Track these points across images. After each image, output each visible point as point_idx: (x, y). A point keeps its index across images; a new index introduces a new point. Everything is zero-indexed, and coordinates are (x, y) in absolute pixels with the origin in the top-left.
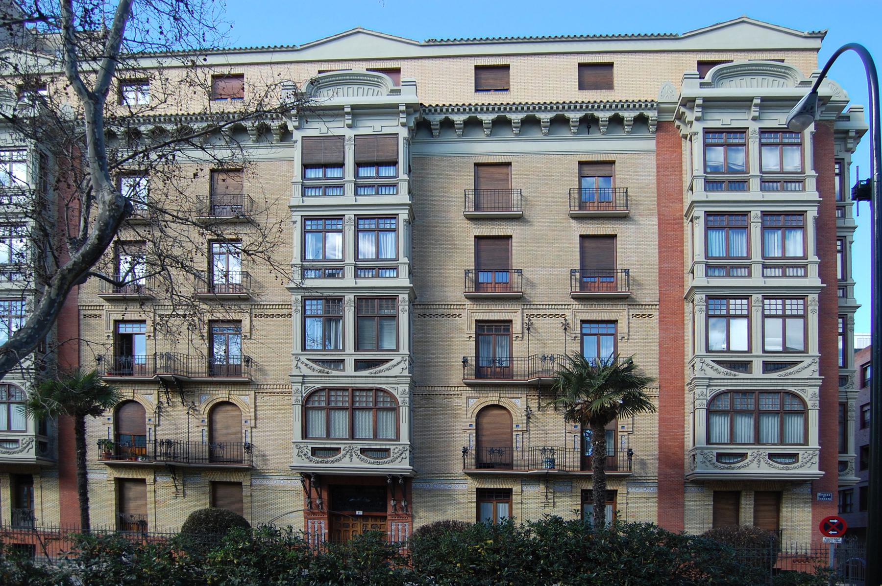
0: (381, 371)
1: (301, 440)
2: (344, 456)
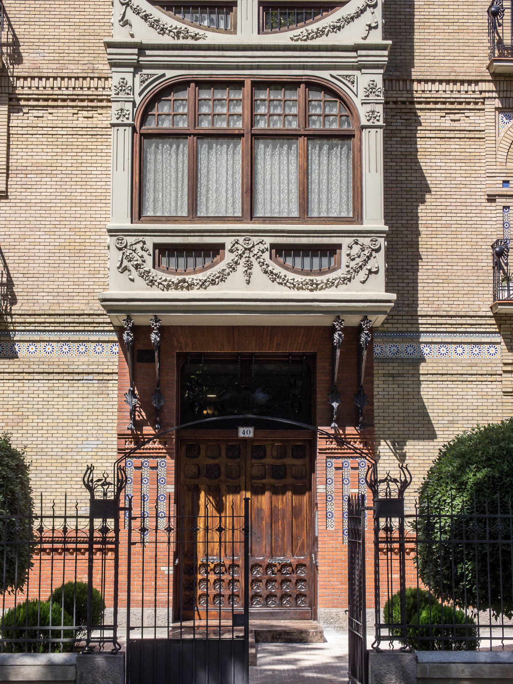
0: (320, 33)
1: (127, 225)
2: (233, 267)
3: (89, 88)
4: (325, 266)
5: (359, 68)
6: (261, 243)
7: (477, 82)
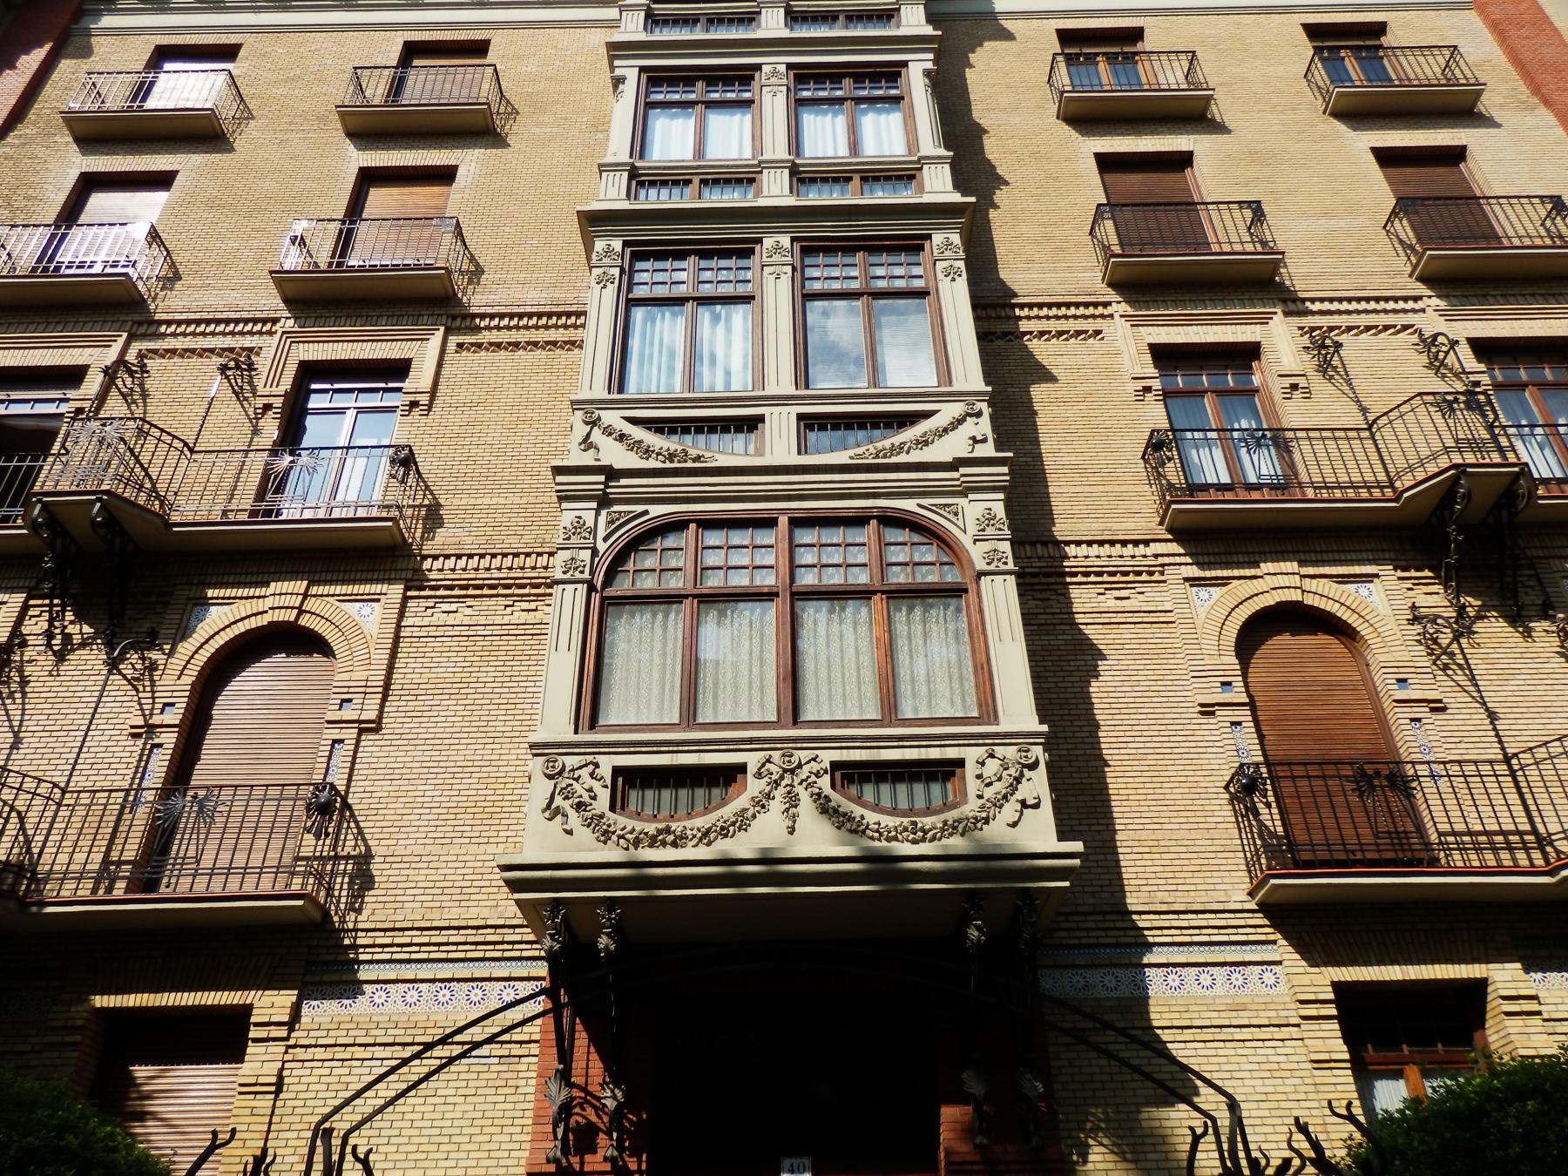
2: (761, 804)
3: (534, 568)
4: (937, 801)
5: (964, 493)
6: (814, 759)
7: (1147, 543)
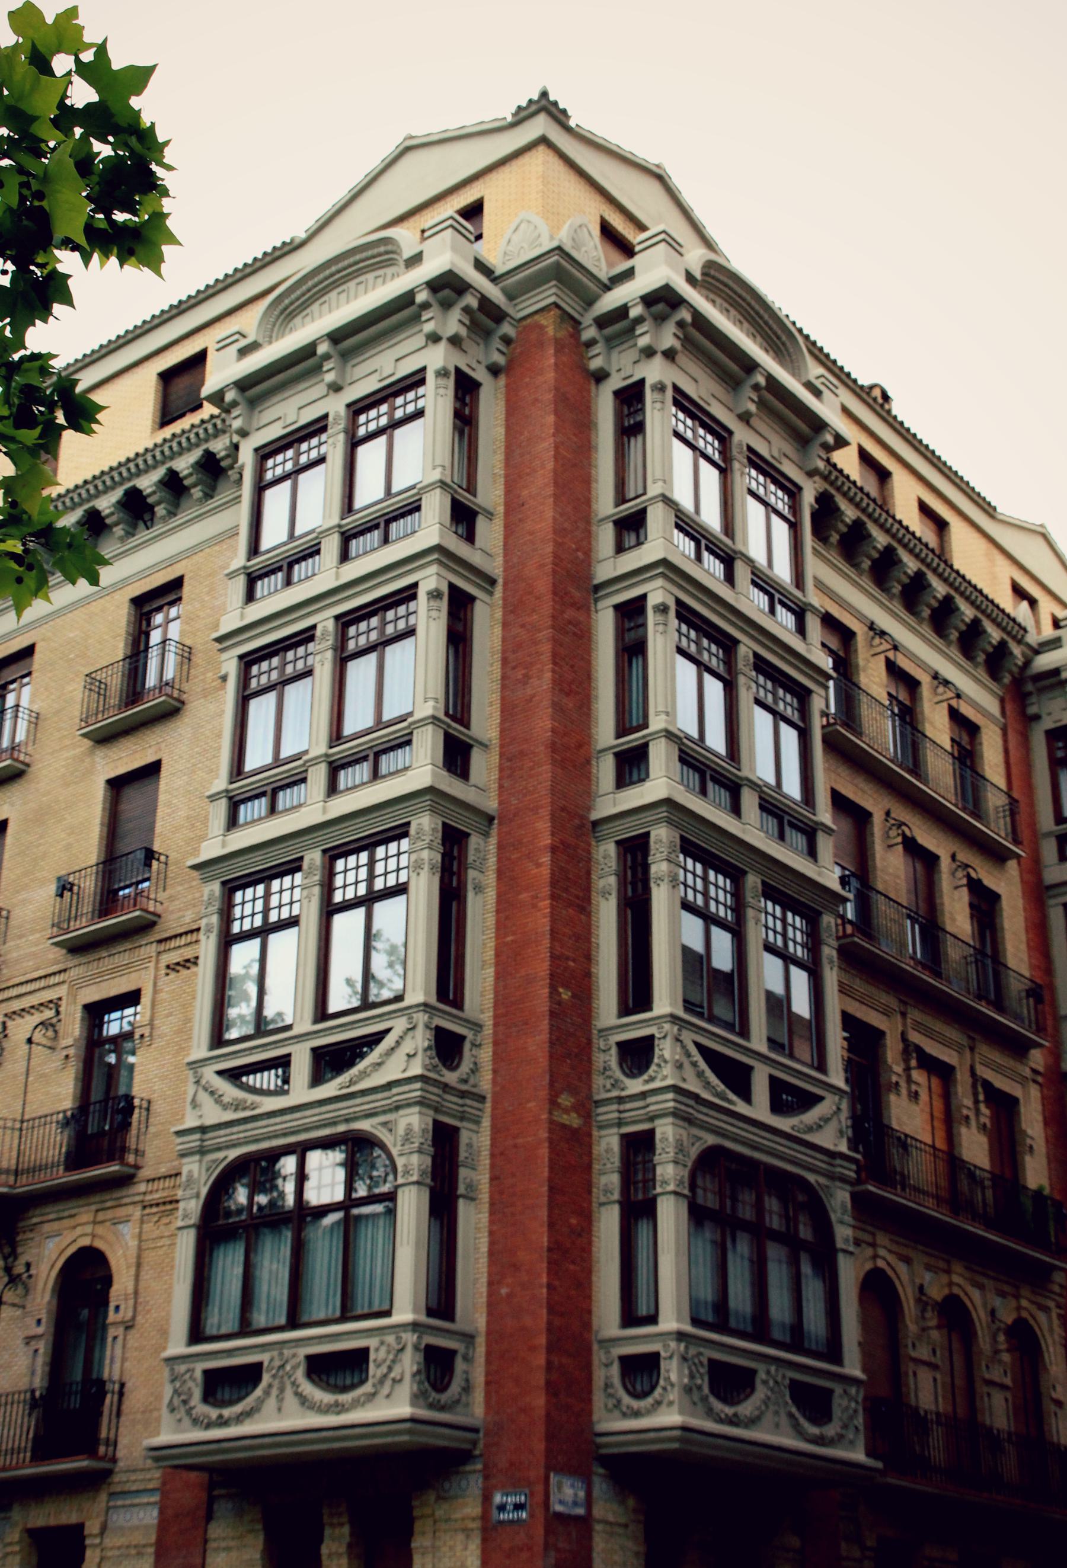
0: (364, 1074)
